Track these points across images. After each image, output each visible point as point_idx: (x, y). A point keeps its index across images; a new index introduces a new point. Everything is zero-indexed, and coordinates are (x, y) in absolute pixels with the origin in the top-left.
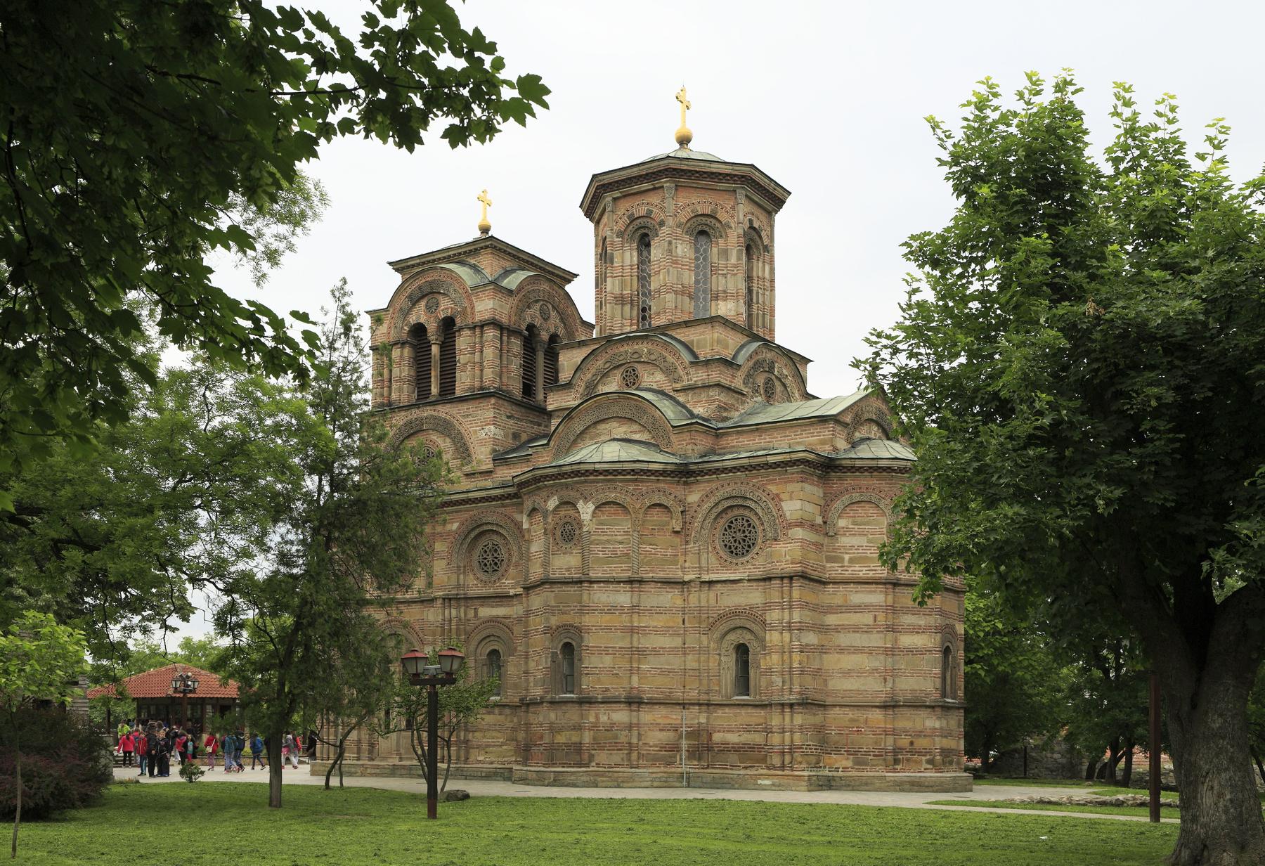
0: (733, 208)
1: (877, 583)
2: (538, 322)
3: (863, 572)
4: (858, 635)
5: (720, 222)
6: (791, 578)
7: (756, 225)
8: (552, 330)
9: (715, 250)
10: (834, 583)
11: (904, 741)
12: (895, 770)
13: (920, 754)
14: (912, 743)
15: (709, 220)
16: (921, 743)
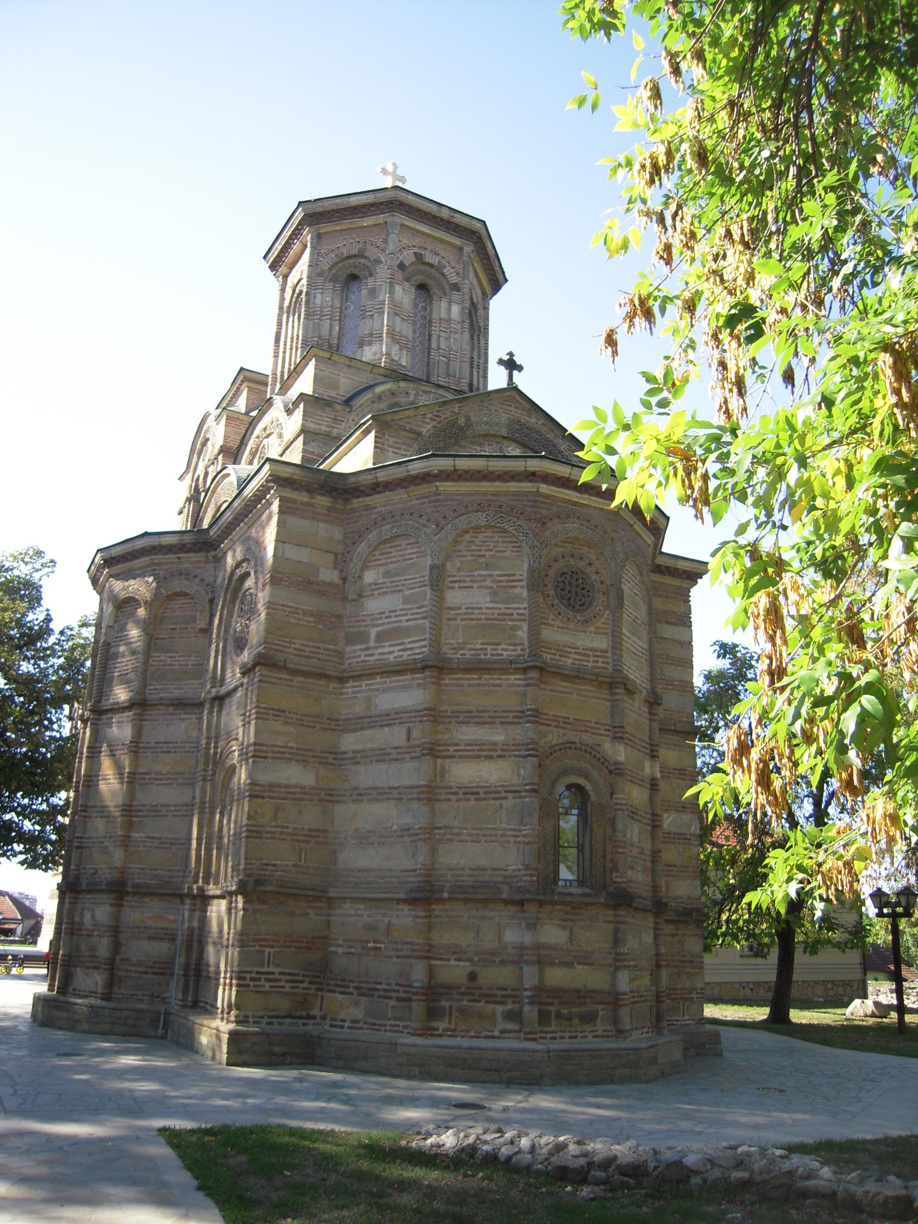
1: (413, 671)
3: (392, 653)
4: (384, 766)
7: (430, 258)
10: (354, 678)
11: (454, 971)
12: (427, 1031)
13: (490, 998)
14: (472, 976)
16: (496, 976)
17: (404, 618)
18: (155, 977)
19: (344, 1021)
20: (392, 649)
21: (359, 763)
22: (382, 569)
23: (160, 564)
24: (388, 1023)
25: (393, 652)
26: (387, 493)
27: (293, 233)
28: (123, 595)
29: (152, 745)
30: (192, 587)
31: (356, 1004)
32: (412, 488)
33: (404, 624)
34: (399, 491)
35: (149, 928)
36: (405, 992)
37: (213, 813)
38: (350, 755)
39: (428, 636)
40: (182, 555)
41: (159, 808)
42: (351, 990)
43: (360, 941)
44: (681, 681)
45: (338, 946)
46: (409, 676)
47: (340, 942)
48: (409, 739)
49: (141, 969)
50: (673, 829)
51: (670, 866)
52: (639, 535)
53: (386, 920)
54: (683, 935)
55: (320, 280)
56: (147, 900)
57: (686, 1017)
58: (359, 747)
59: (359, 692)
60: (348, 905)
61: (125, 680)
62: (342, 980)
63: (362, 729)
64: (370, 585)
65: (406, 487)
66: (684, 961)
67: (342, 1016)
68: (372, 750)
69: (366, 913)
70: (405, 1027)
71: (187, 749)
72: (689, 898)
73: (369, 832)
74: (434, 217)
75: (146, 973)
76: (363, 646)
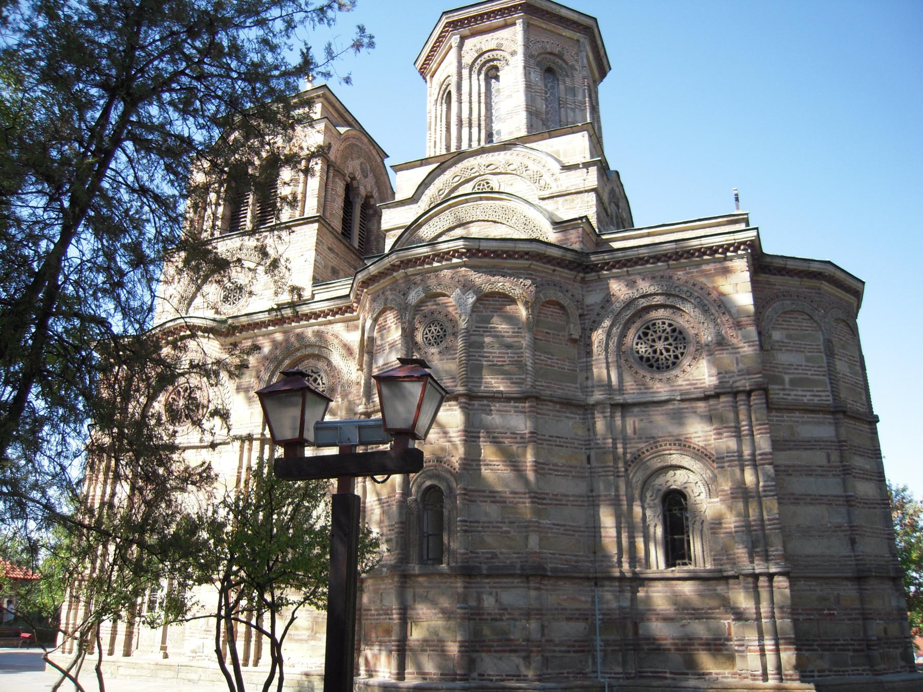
0: (577, 54)
2: (358, 175)
3: (806, 396)
4: (812, 479)
5: (566, 63)
6: (749, 393)
8: (369, 189)
9: (562, 87)
14: (885, 631)
15: (557, 60)
17: (809, 373)
18: (575, 655)
19: (813, 671)
20: (804, 393)
21: (791, 475)
22: (785, 332)
23: (535, 270)
24: (849, 669)
25: (805, 396)
26: (787, 277)
27: (500, 10)
28: (487, 288)
29: (547, 437)
30: (565, 302)
31: (821, 657)
32: (805, 279)
33: (811, 377)
34: (796, 278)
35: (565, 609)
36: (859, 645)
37: (630, 506)
38: (783, 469)
39: (829, 388)
40: (558, 269)
41: (559, 497)
42: (816, 647)
43: (816, 609)
45: (800, 614)
46: (821, 416)
47: (800, 611)
48: (829, 461)
49: (563, 649)
53: (836, 593)
55: (532, 61)
56: (561, 583)
58: (790, 463)
59: (782, 421)
60: (802, 582)
61: (497, 370)
62: (807, 640)
63: (790, 449)
64: (778, 342)
65: (801, 278)
67: (811, 667)
68: (800, 466)
69: (818, 588)
70: (863, 670)
71: (576, 445)
73: (808, 527)
75: (569, 652)
76: (781, 387)
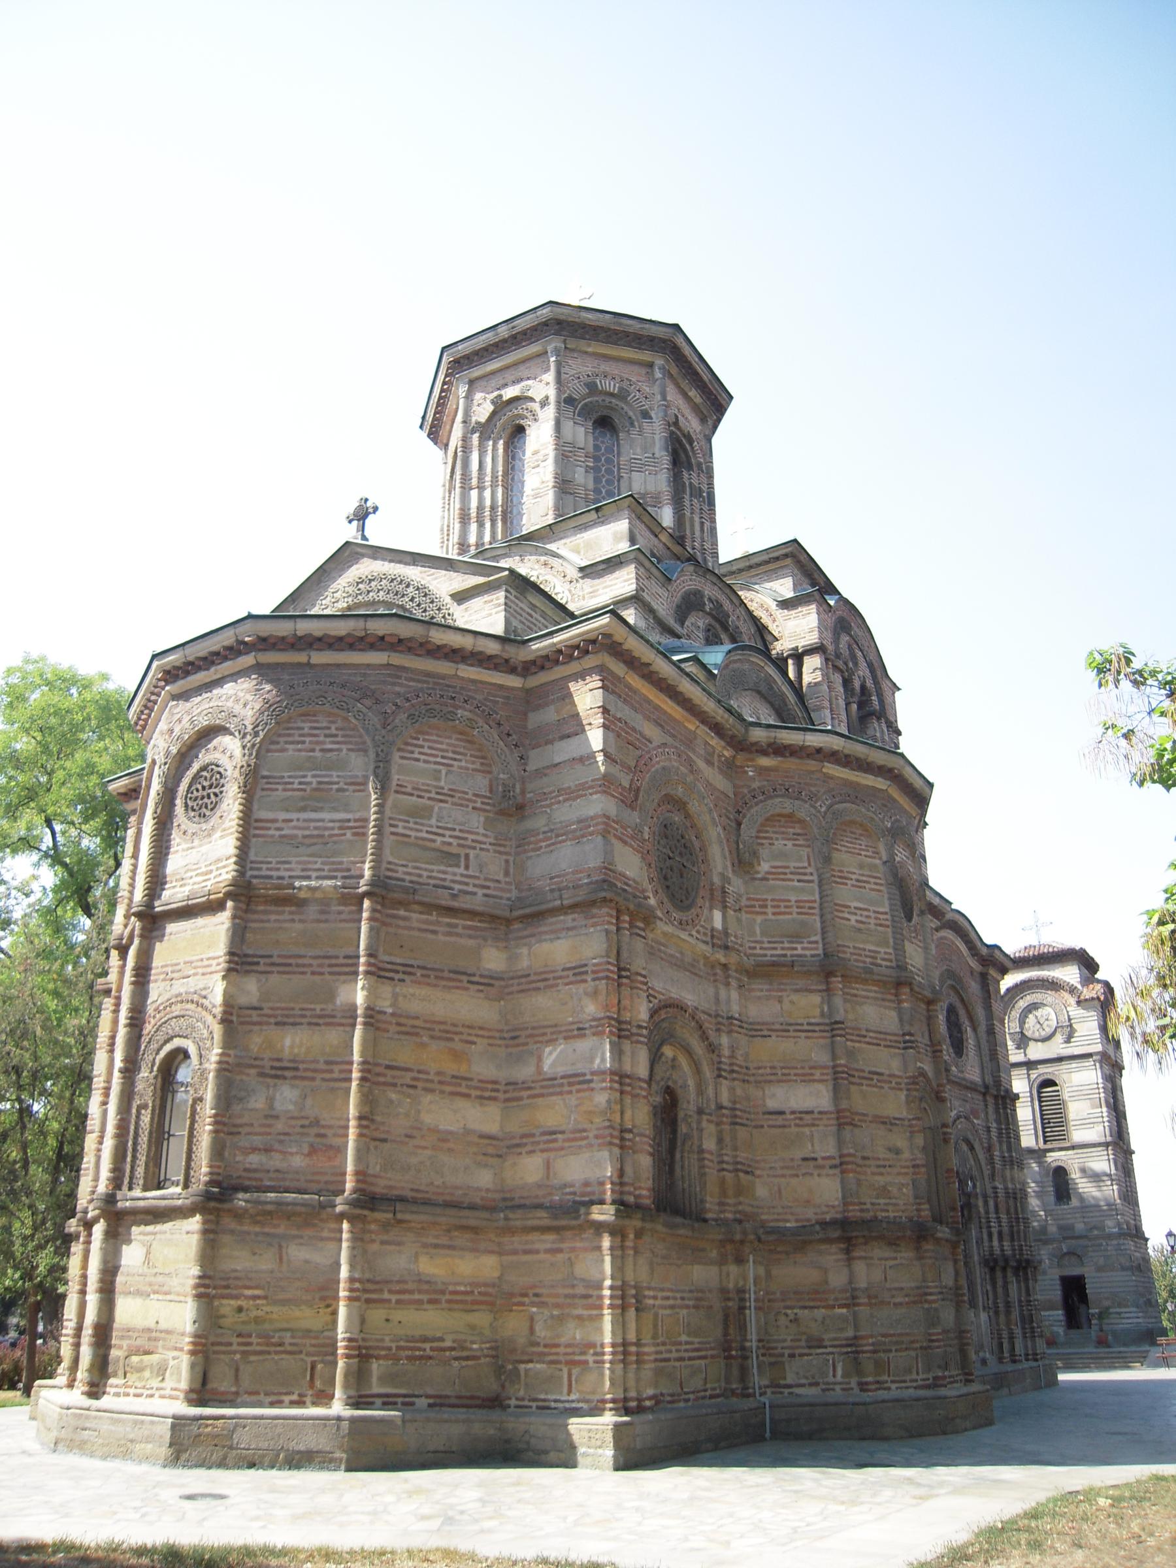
44: (580, 821)
50: (561, 1070)
51: (554, 1133)
52: (338, 666)
54: (573, 1249)
57: (573, 1397)
66: (574, 1296)
72: (586, 1184)
74: (496, 345)
